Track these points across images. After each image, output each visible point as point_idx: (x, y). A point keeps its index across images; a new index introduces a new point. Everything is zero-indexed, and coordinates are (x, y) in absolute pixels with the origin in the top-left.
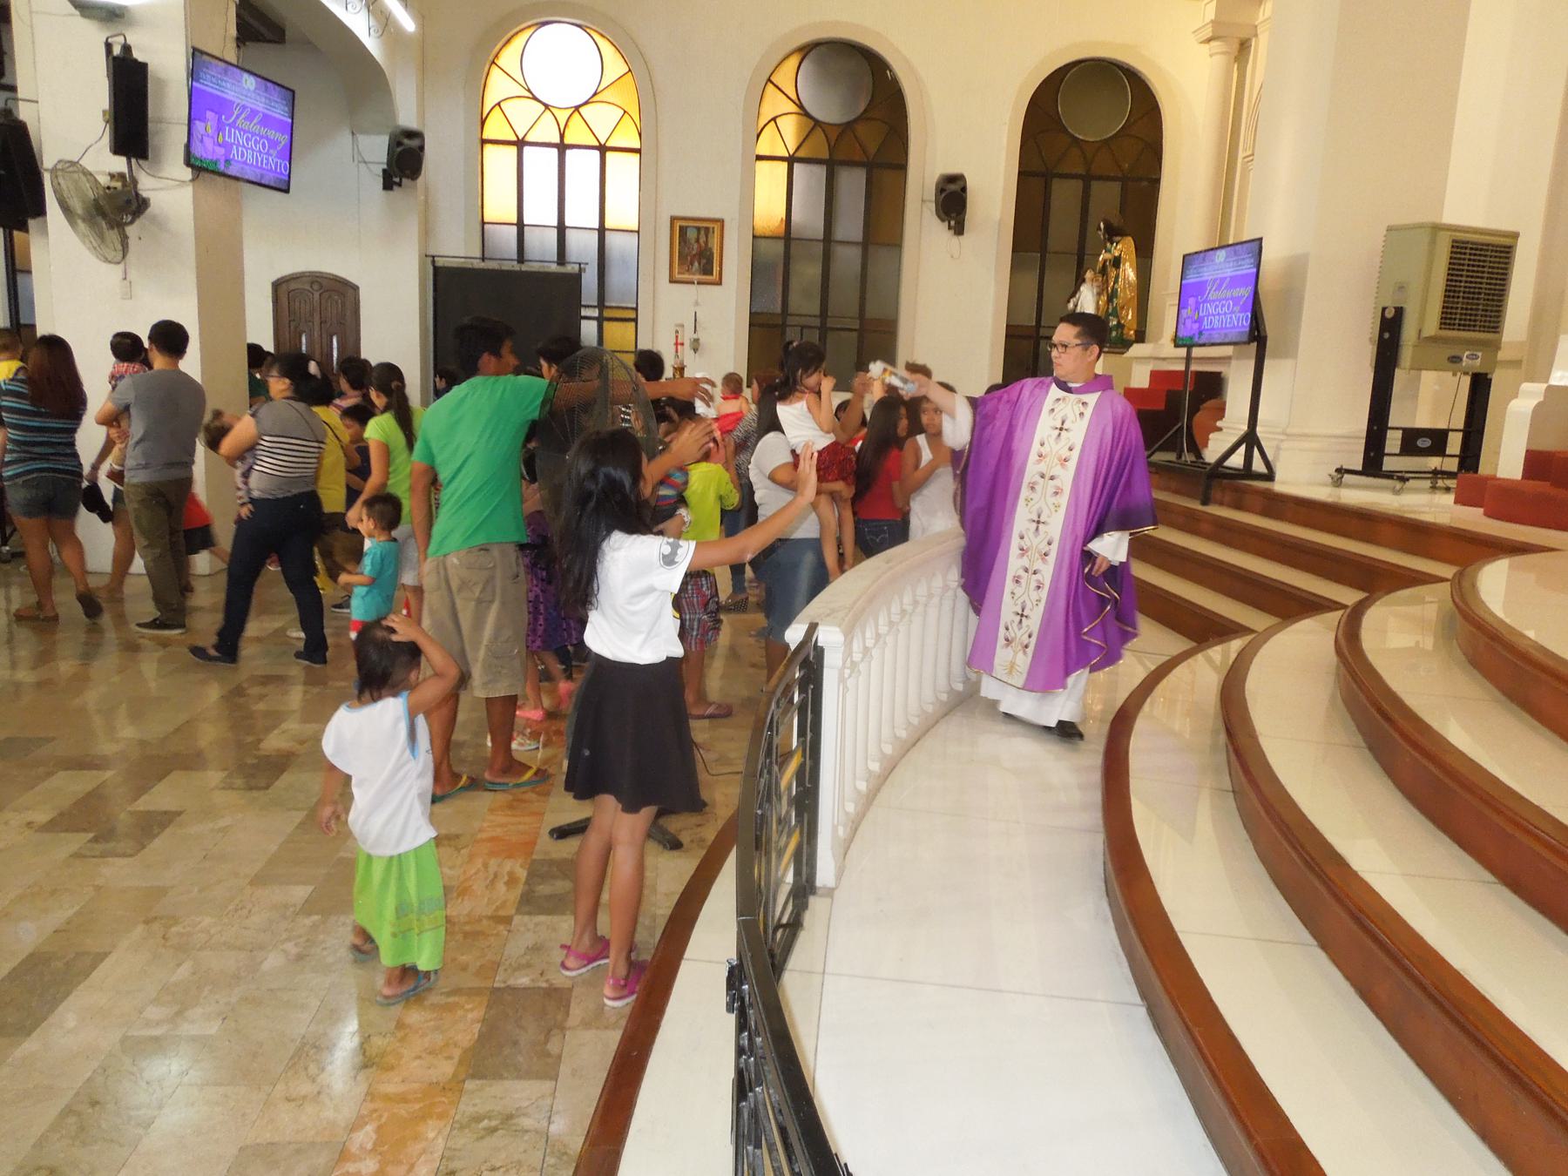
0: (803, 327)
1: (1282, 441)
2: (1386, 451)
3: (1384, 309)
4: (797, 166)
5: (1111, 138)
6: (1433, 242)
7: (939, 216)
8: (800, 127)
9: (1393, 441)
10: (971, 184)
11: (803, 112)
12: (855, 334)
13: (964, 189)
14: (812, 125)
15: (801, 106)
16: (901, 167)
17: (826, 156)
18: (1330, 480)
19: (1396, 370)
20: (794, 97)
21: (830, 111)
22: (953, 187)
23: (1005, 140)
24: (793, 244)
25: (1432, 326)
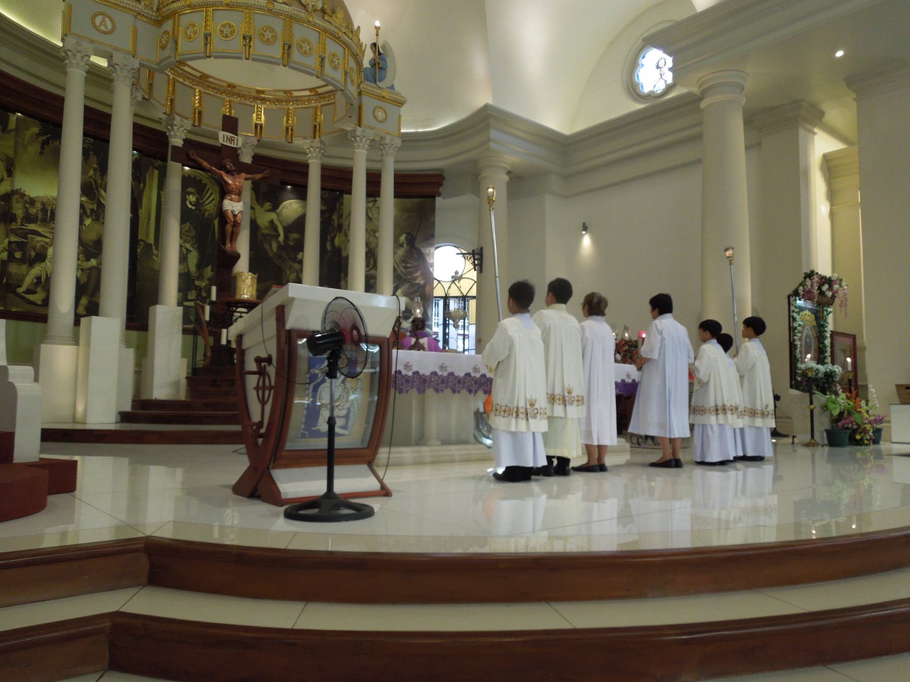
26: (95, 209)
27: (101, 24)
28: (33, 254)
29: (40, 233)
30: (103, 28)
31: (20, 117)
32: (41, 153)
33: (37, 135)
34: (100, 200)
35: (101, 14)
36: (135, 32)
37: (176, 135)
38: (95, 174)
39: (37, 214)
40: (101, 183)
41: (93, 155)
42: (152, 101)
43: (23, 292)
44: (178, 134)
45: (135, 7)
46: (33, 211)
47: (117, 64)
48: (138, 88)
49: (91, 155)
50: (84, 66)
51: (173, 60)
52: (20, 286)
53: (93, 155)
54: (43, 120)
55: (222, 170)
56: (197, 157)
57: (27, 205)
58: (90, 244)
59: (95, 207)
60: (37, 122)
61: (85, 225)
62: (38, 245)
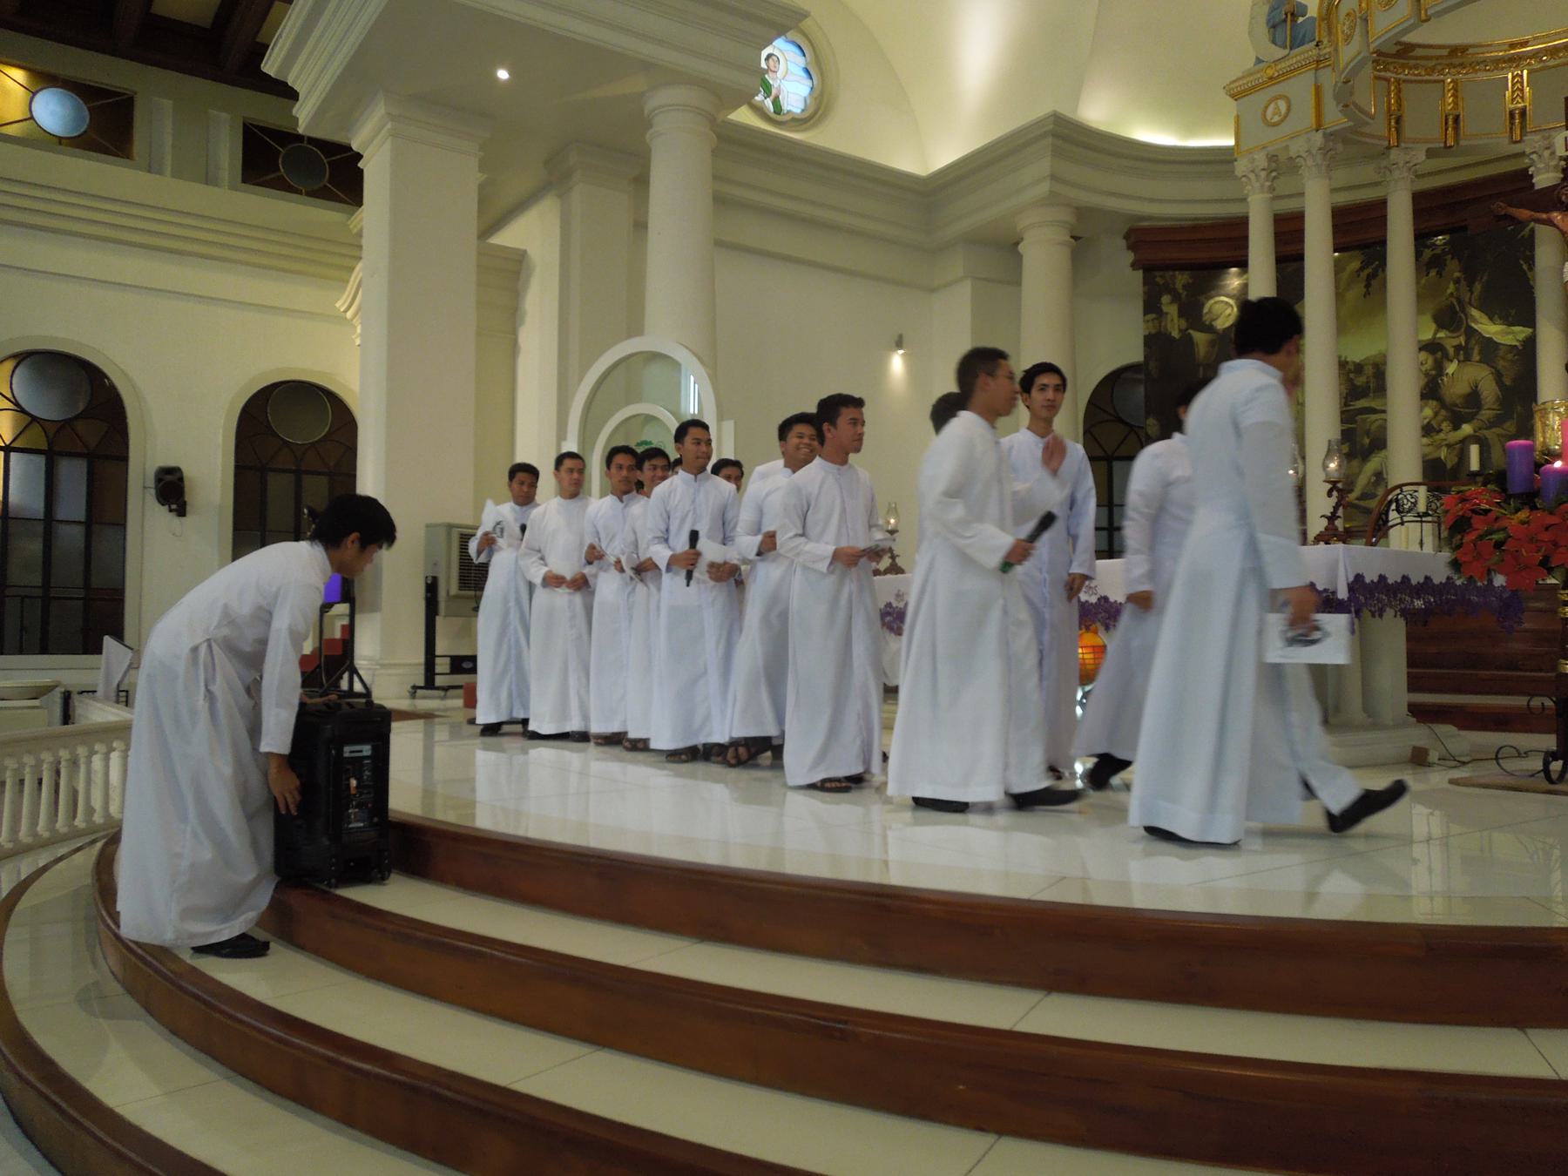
0: (23, 598)
1: (376, 669)
2: (437, 671)
3: (427, 577)
4: (13, 455)
5: (316, 442)
6: (449, 534)
7: (159, 502)
8: (16, 422)
9: (442, 665)
10: (187, 472)
11: (19, 408)
12: (80, 603)
13: (181, 479)
14: (27, 420)
15: (16, 404)
16: (124, 458)
17: (45, 447)
18: (408, 694)
19: (437, 618)
20: (9, 396)
21: (47, 408)
22: (169, 478)
23: (220, 439)
24: (11, 523)
25: (454, 590)
26: (1463, 343)
27: (1274, 114)
28: (1367, 441)
29: (1375, 409)
30: (1276, 119)
31: (1338, 257)
32: (1367, 294)
33: (1357, 271)
34: (1472, 328)
35: (1270, 102)
36: (1318, 90)
37: (1538, 170)
38: (1457, 289)
39: (1367, 382)
40: (1470, 300)
41: (1452, 259)
42: (1463, 143)
43: (1357, 499)
44: (1541, 166)
45: (1300, 62)
46: (1360, 381)
47: (1298, 156)
48: (1408, 145)
49: (1448, 262)
50: (1262, 186)
51: (1340, 108)
52: (1351, 491)
53: (1452, 259)
54: (1362, 247)
55: (1557, 209)
56: (1508, 208)
57: (1352, 376)
58: (1458, 402)
59: (1462, 340)
60: (1356, 253)
61: (1447, 374)
62: (1373, 427)
